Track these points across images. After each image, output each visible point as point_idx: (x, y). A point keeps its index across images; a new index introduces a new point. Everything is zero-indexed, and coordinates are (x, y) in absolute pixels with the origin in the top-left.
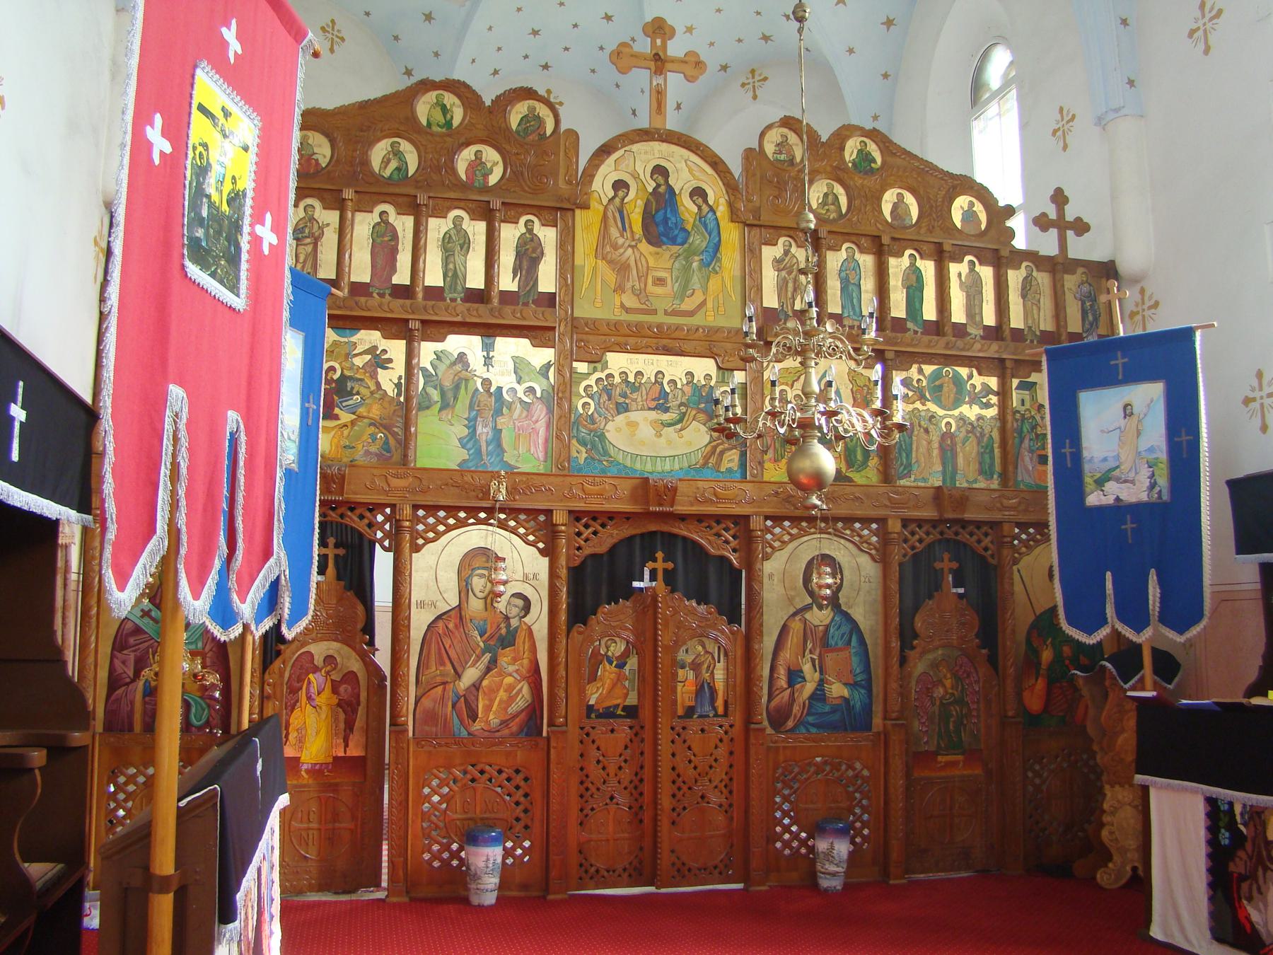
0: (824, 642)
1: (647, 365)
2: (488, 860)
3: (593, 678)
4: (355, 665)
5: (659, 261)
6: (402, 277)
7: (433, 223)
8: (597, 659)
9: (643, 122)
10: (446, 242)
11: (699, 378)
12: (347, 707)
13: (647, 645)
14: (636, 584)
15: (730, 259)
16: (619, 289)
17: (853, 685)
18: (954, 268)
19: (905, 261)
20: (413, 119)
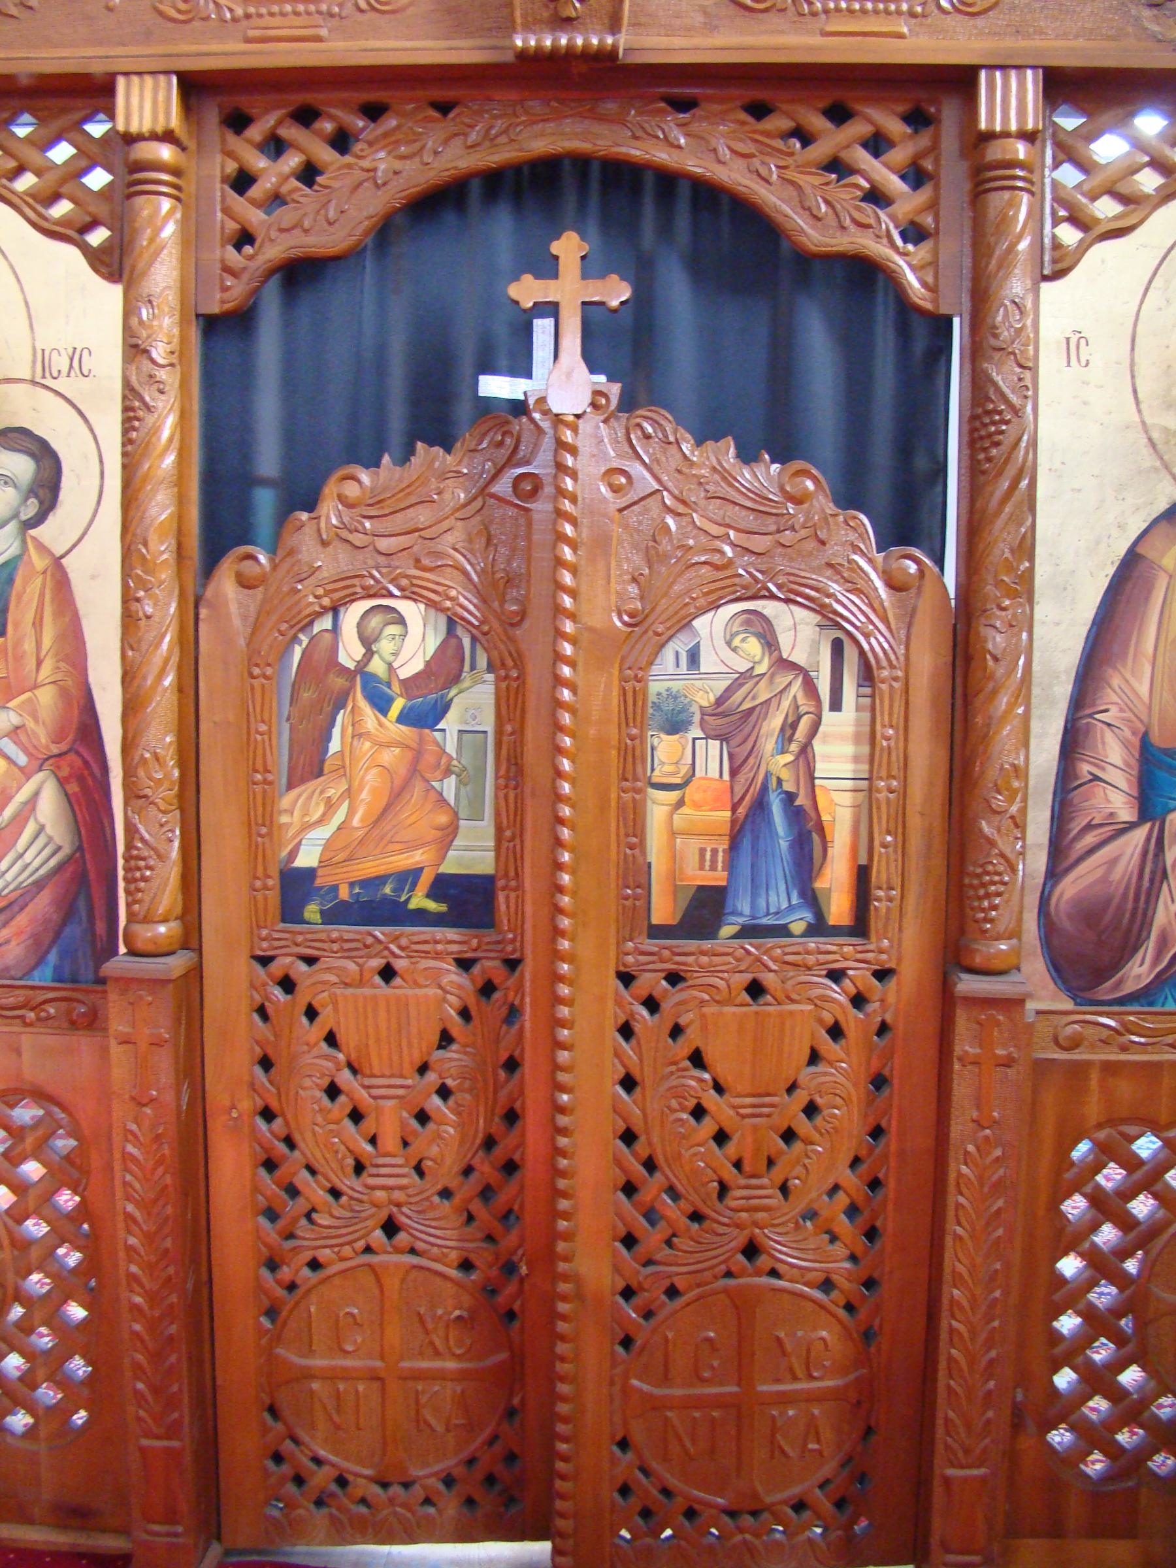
3: (310, 764)
13: (504, 629)
14: (496, 387)
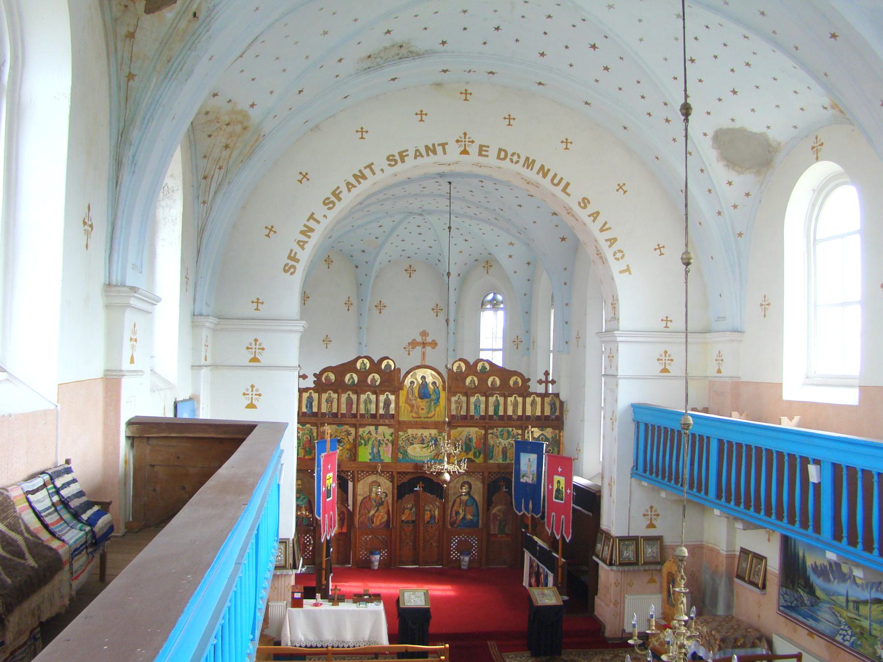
0: (466, 504)
1: (419, 432)
4: (344, 510)
5: (423, 404)
6: (354, 411)
7: (362, 396)
8: (404, 509)
10: (365, 400)
11: (433, 435)
13: (417, 504)
15: (443, 401)
16: (412, 412)
18: (509, 399)
19: (494, 398)
20: (356, 368)
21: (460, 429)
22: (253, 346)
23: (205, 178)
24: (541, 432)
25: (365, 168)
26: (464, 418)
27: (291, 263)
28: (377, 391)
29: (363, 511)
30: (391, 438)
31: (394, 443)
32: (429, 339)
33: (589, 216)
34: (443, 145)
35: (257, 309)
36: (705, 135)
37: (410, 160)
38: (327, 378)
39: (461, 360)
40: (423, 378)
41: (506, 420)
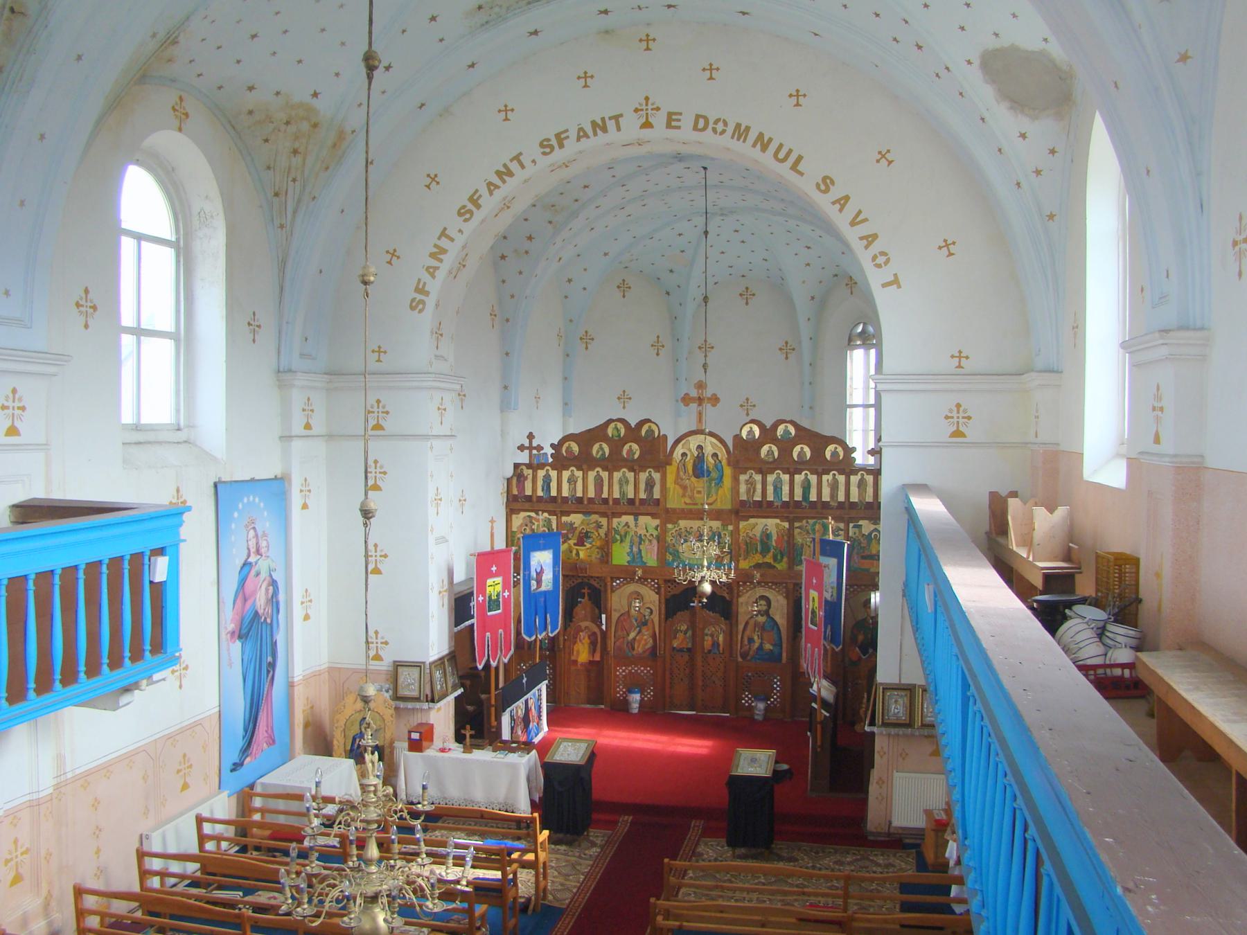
0: (763, 628)
1: (695, 524)
2: (636, 697)
4: (596, 630)
5: (699, 484)
6: (605, 495)
8: (677, 631)
9: (694, 428)
10: (620, 480)
11: (715, 529)
12: (593, 644)
13: (692, 626)
16: (684, 496)
17: (774, 645)
18: (825, 478)
21: (752, 521)
22: (375, 409)
23: (276, 195)
24: (872, 527)
25: (511, 160)
26: (758, 504)
27: (419, 297)
28: (636, 466)
29: (619, 633)
30: (655, 533)
31: (661, 539)
32: (708, 393)
33: (834, 203)
34: (616, 118)
35: (379, 361)
36: (969, 62)
37: (571, 146)
38: (569, 450)
39: (753, 421)
40: (700, 447)
41: (820, 509)
